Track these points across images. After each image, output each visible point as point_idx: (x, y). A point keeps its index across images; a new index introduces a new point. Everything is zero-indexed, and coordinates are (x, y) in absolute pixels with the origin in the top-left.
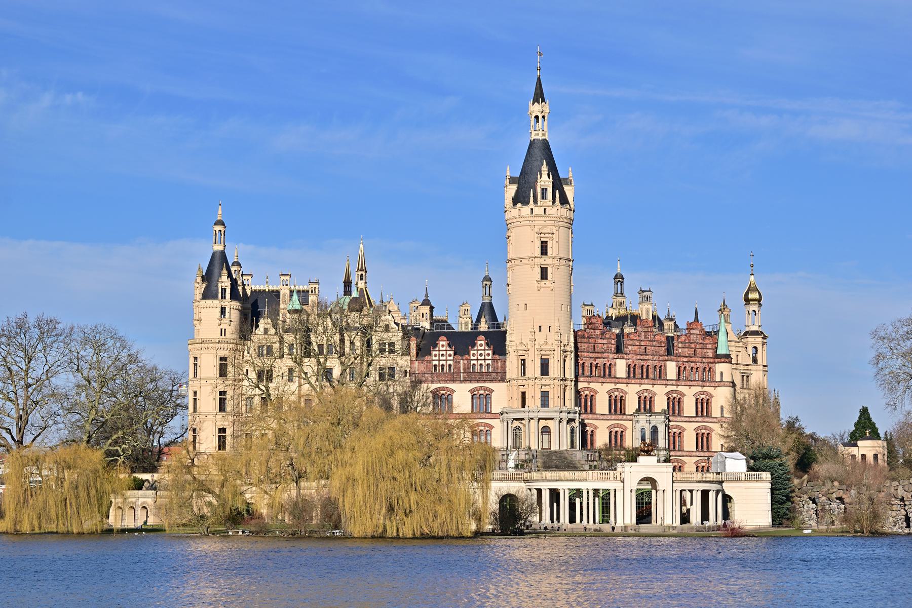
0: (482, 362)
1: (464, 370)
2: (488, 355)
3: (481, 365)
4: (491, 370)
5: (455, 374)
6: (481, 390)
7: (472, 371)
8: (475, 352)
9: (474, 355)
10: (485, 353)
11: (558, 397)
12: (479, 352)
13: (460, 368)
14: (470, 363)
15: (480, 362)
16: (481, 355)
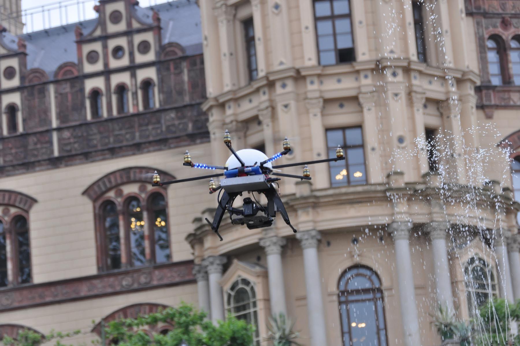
0: (125, 78)
1: (61, 116)
2: (144, 47)
3: (121, 89)
4: (156, 102)
5: (32, 140)
6: (129, 182)
7: (89, 117)
8: (97, 47)
9: (92, 57)
10: (131, 43)
11: (401, 140)
12: (112, 44)
13: (46, 111)
14: (82, 90)
15: (116, 79)
16: (118, 51)
